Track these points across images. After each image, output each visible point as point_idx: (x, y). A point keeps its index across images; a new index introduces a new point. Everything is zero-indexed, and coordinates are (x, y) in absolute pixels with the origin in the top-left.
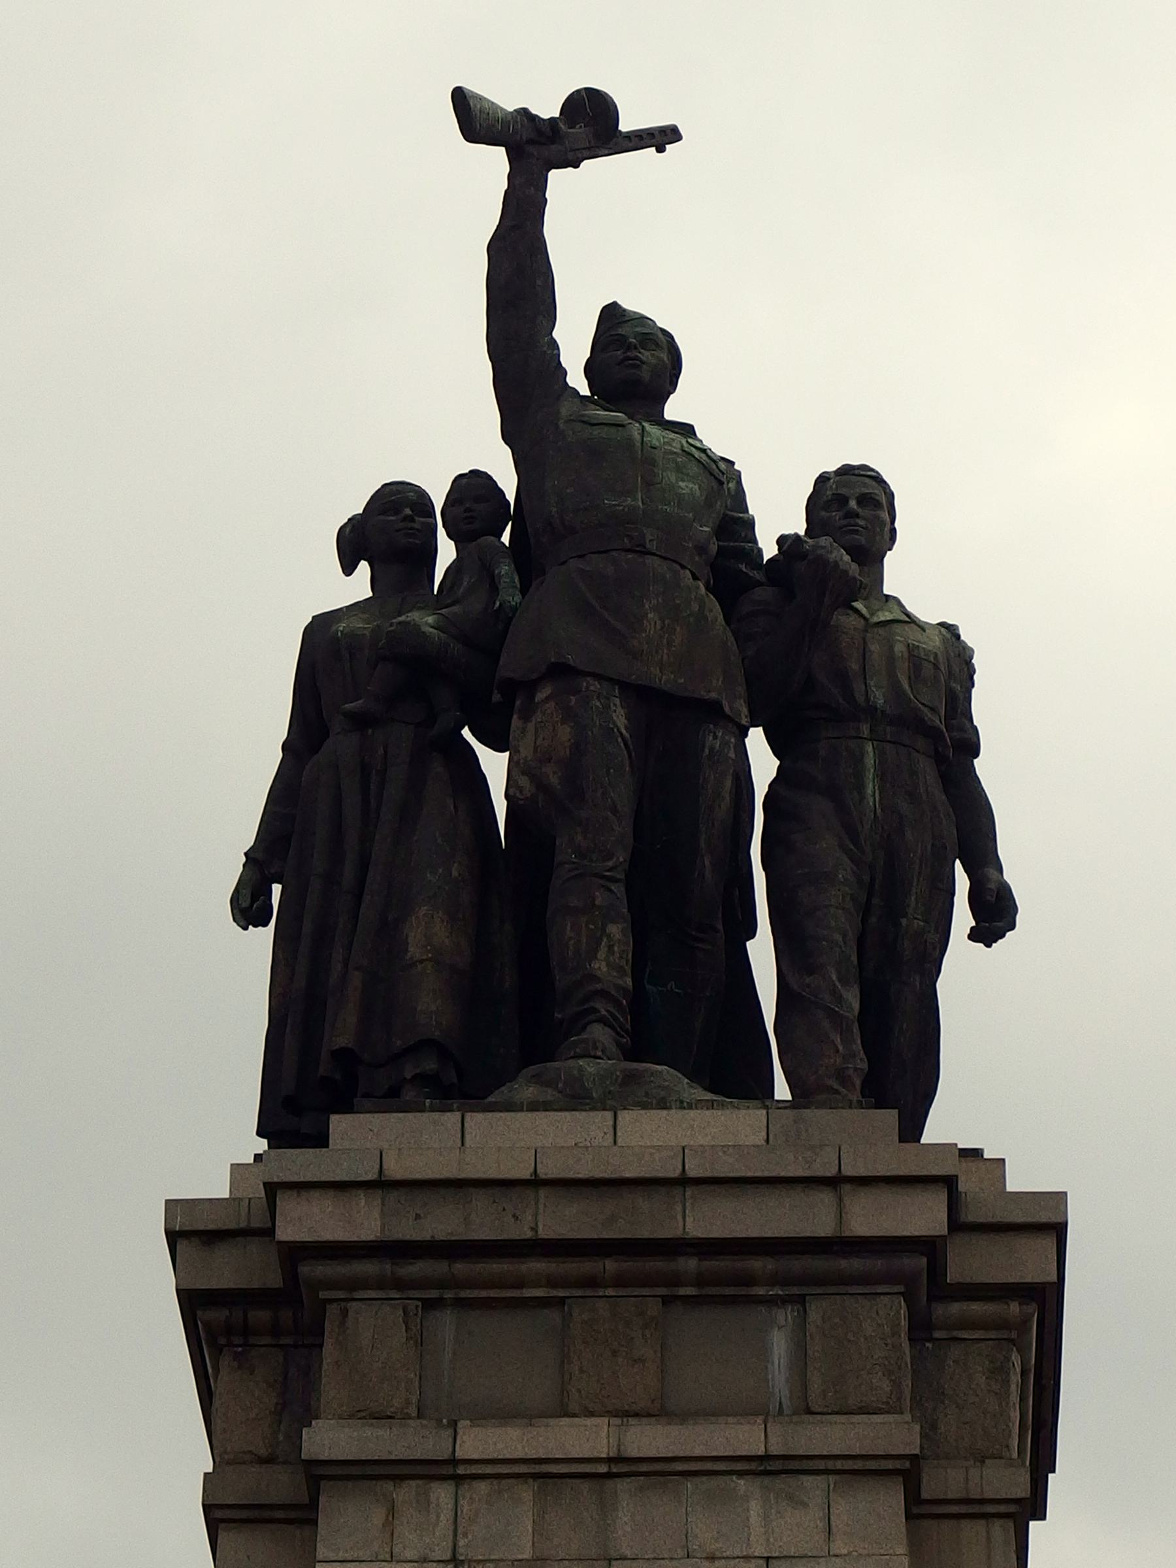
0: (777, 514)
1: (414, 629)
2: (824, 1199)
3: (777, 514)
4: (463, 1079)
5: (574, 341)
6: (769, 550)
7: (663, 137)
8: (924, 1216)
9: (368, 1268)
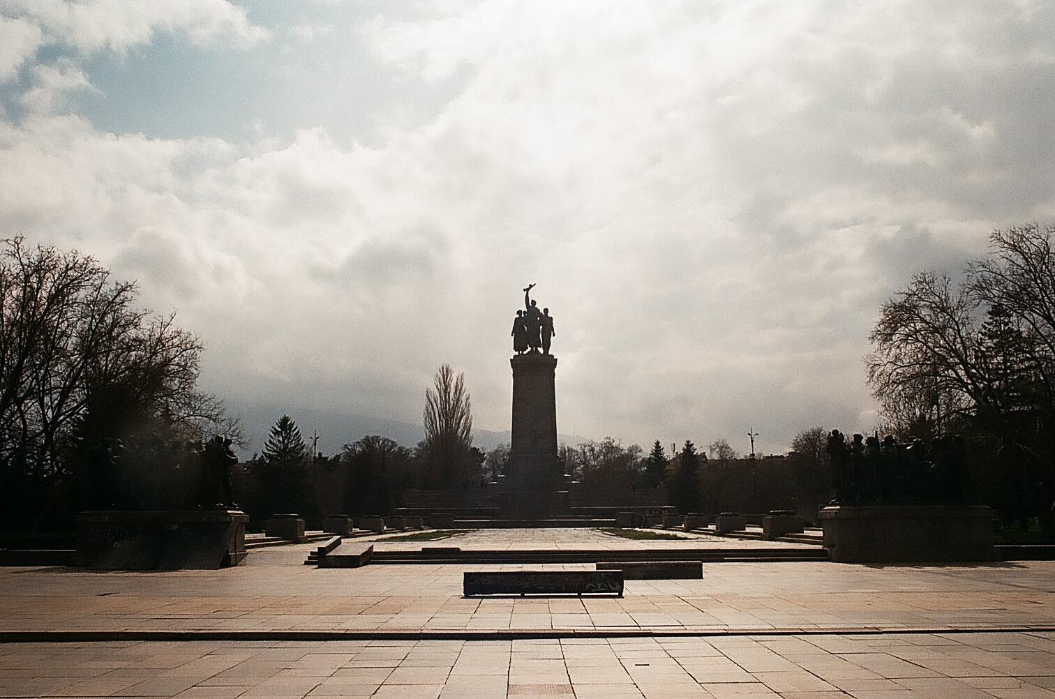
3: (542, 311)
5: (530, 302)
7: (535, 285)
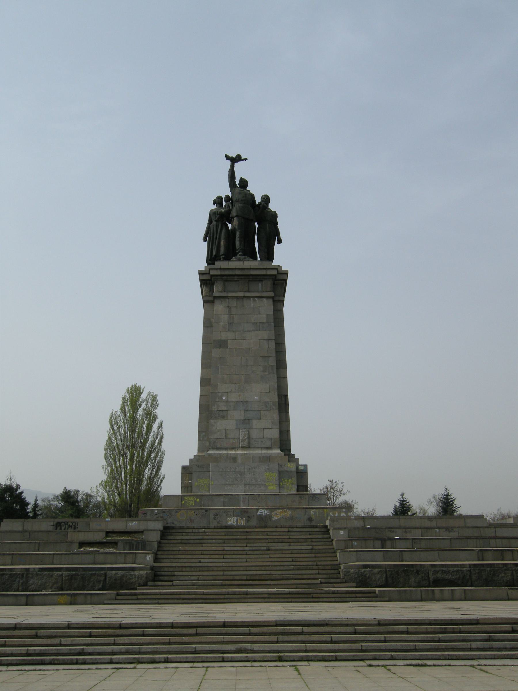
0: (258, 200)
1: (221, 211)
2: (265, 271)
3: (258, 200)
4: (227, 258)
5: (237, 181)
6: (257, 203)
7: (246, 159)
8: (274, 272)
9: (219, 277)
